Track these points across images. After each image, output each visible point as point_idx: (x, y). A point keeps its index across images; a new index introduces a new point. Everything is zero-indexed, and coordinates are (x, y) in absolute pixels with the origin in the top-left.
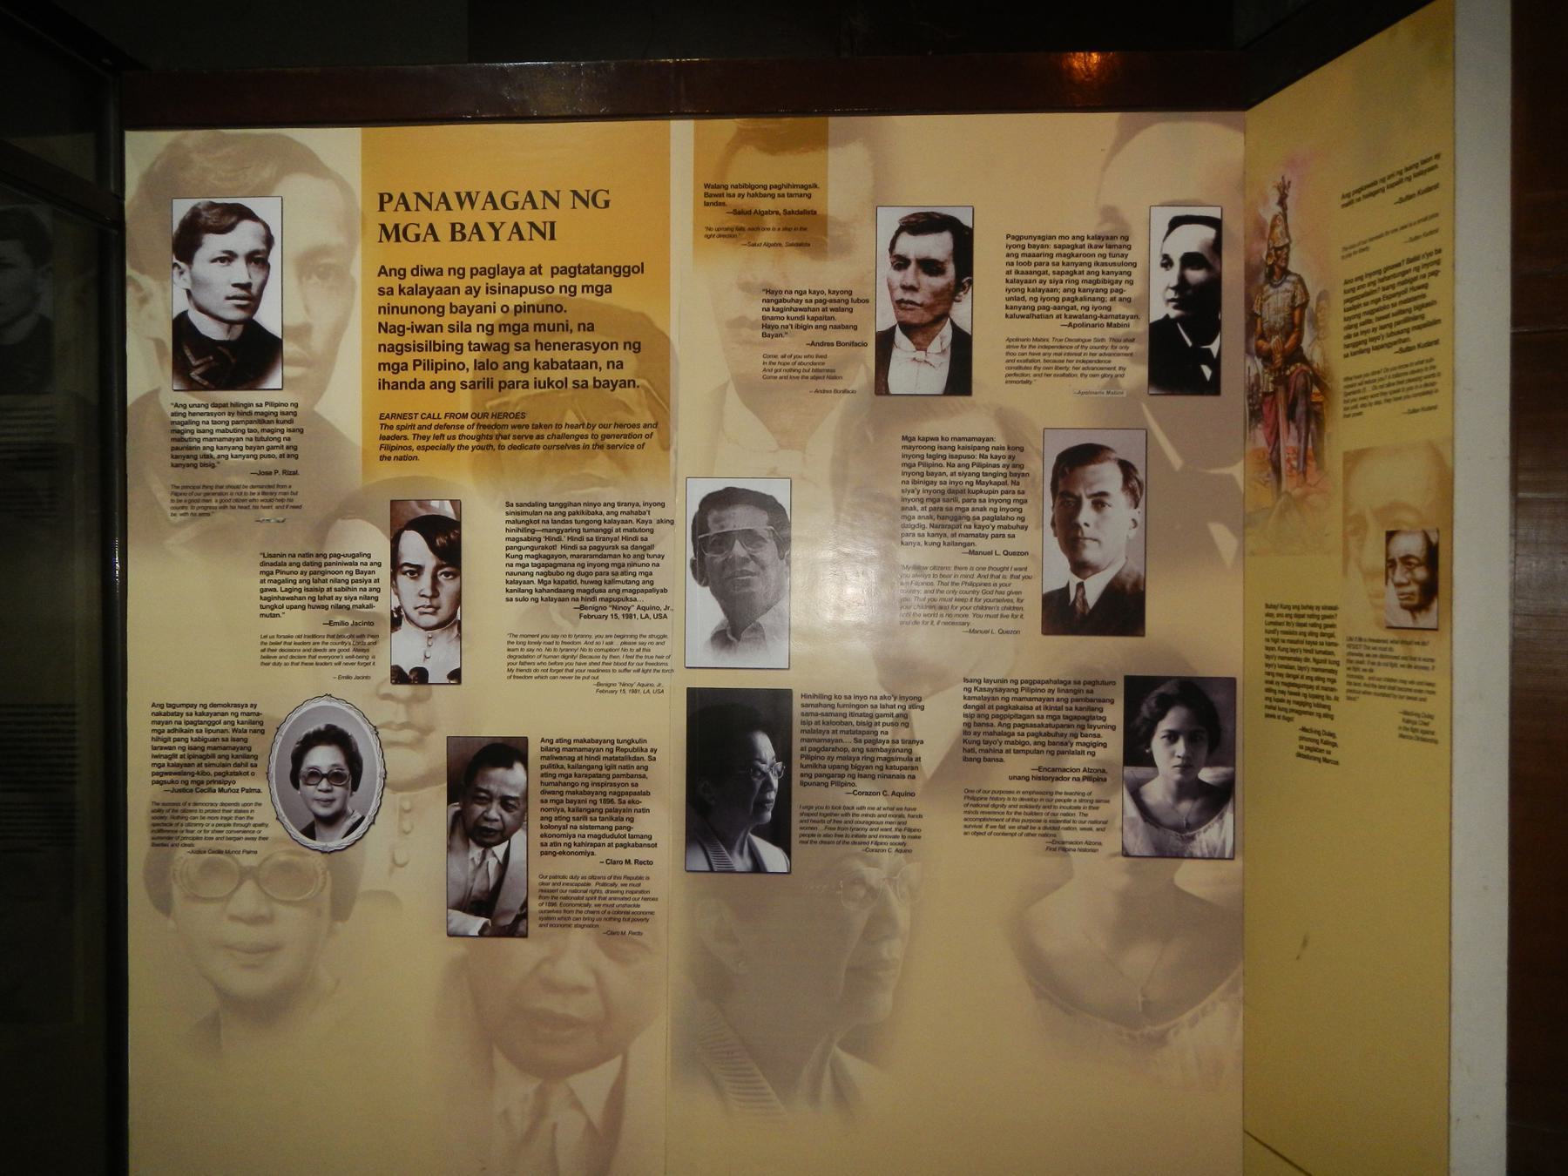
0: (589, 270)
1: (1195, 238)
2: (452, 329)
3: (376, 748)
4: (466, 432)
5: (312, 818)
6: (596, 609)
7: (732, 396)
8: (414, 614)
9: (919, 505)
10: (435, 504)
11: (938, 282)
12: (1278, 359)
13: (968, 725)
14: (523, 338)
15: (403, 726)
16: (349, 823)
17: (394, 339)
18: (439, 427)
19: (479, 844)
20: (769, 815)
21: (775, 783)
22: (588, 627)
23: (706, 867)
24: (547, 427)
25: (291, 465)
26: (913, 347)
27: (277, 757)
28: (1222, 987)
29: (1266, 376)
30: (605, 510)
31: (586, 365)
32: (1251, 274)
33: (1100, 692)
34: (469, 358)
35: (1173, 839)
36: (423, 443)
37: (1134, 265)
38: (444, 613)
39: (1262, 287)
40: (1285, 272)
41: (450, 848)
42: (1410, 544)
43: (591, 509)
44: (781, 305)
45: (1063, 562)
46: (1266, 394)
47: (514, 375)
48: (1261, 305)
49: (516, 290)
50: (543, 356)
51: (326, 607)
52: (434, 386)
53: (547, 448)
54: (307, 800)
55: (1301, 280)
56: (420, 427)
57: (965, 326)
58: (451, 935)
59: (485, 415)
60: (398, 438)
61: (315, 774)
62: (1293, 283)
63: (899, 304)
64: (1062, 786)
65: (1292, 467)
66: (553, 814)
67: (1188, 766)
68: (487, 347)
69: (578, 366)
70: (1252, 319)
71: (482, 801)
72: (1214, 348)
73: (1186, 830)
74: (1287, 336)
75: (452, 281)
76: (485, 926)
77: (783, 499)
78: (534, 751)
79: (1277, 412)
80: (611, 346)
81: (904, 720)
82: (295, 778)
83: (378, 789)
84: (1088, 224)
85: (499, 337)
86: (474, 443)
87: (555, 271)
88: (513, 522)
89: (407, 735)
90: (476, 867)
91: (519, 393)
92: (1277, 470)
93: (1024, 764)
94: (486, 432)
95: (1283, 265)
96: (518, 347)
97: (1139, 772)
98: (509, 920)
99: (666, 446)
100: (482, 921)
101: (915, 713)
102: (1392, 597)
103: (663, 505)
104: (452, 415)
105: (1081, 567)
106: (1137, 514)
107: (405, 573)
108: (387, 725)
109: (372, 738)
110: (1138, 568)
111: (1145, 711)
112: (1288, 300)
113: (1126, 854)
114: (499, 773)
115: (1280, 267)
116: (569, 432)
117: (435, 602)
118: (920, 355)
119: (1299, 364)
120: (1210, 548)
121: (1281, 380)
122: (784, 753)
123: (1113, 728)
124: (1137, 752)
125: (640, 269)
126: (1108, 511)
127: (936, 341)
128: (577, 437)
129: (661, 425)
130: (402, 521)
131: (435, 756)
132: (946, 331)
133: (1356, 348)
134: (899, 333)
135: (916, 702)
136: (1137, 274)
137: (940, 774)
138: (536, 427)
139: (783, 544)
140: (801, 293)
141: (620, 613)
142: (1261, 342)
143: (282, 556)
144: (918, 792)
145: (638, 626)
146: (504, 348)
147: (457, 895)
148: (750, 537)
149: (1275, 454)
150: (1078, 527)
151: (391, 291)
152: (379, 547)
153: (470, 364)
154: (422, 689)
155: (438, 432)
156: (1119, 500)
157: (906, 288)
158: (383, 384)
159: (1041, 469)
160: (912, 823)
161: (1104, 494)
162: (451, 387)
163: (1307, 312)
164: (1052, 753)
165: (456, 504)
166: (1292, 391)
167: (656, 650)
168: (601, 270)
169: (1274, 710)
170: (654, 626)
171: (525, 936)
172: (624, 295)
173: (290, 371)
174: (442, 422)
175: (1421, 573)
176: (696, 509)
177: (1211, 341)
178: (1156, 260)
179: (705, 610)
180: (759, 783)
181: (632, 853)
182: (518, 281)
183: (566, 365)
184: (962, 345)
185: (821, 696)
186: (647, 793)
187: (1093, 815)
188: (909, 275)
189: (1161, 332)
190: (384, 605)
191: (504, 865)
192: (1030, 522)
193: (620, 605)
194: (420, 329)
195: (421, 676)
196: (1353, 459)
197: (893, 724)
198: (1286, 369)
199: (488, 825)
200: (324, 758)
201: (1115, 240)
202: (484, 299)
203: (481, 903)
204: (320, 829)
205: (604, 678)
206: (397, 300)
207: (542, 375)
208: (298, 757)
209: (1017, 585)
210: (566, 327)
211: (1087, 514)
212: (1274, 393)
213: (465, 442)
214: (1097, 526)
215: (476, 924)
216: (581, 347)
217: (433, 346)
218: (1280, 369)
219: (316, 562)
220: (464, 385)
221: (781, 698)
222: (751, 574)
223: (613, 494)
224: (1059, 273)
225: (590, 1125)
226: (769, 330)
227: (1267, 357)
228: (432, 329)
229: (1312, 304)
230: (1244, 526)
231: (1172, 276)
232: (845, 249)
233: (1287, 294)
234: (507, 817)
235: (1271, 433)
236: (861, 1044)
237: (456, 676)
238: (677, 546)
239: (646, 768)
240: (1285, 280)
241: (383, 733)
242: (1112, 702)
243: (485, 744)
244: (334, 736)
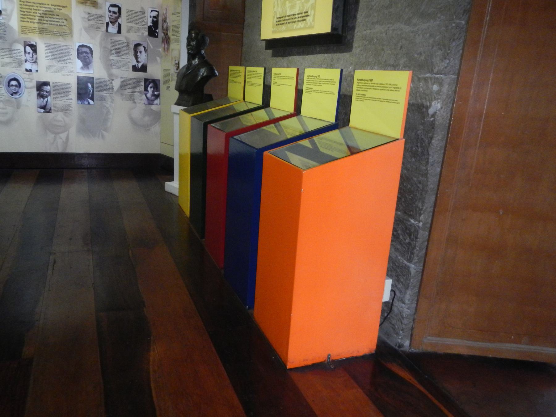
0: (58, 6)
1: (155, 14)
2: (34, 13)
3: (23, 82)
4: (37, 31)
5: (12, 93)
6: (61, 62)
7: (83, 31)
8: (29, 60)
9: (113, 50)
10: (32, 42)
11: (116, 15)
12: (165, 34)
13: (121, 84)
14: (46, 16)
15: (28, 78)
16: (19, 94)
17: (23, 13)
18: (32, 29)
19: (42, 98)
20: (90, 96)
21: (91, 91)
22: (60, 65)
23: (81, 103)
24: (51, 31)
25: (5, 33)
26: (112, 25)
27: (5, 82)
28: (157, 123)
30: (62, 46)
31: (58, 22)
32: (163, 21)
33: (141, 80)
34: (37, 18)
35: (151, 102)
36: (29, 31)
37: (146, 17)
38: (34, 60)
41: (37, 99)
42: (177, 62)
43: (59, 46)
44: (91, 16)
45: (135, 61)
47: (45, 22)
49: (45, 8)
50: (50, 19)
51: (12, 58)
52: (31, 22)
53: (52, 35)
54: (11, 89)
55: (168, 24)
56: (29, 29)
57: (120, 22)
58: (38, 112)
59: (40, 28)
60: (24, 30)
61: (12, 85)
63: (110, 18)
64: (135, 94)
66: (55, 94)
67: (153, 92)
68: (40, 17)
69: (56, 22)
70: (163, 27)
71: (42, 91)
72: (157, 31)
73: (153, 101)
75: (33, 5)
76: (44, 111)
77: (92, 47)
78: (51, 84)
80: (62, 19)
81: (111, 83)
82: (9, 86)
83: (24, 88)
84: (139, 9)
85: (42, 15)
86: (38, 33)
87: (52, 5)
88: (46, 47)
89: (29, 80)
90: (42, 102)
91: (46, 25)
92: (165, 50)
93: (130, 90)
94: (41, 31)
96: (46, 17)
97: (147, 92)
98: (48, 110)
99: (72, 36)
100: (44, 110)
101: (113, 82)
102: (175, 69)
103: (71, 46)
104: (34, 28)
105: (138, 62)
106: (146, 54)
107: (27, 53)
108: (25, 78)
109: (22, 80)
110: (146, 63)
111: (147, 83)
113: (144, 104)
114: (45, 87)
116: (56, 33)
117: (33, 58)
118: (113, 27)
120: (156, 60)
121: (166, 37)
122: (93, 87)
123: (142, 86)
124: (146, 89)
125: (67, 7)
126: (142, 54)
127: (116, 25)
128: (57, 34)
129: (71, 33)
130: (26, 44)
131: (34, 84)
132: (117, 23)
133: (173, 35)
134: (110, 23)
135: (113, 80)
136: (146, 18)
137: (117, 91)
138: (50, 31)
139: (92, 54)
140: (94, 14)
141: (65, 63)
143: (4, 48)
144: (113, 93)
145: (68, 65)
146: (43, 17)
147: (39, 106)
148: (86, 53)
150: (137, 56)
151: (22, 5)
152: (22, 49)
153: (37, 19)
154: (31, 73)
155: (32, 30)
156: (143, 52)
157: (111, 16)
158: (21, 21)
159: (132, 47)
160: (113, 98)
161: (141, 51)
162: (34, 23)
164: (134, 89)
165: (36, 43)
167: (71, 69)
168: (60, 6)
169: (164, 84)
170: (71, 65)
171: (51, 113)
172: (64, 11)
173: (3, 16)
174: (32, 28)
175: (178, 65)
176: (77, 47)
177: (157, 30)
178: (149, 16)
179: (79, 64)
180: (89, 91)
181: (68, 101)
182: (45, 6)
183: (54, 21)
184: (120, 26)
185: (99, 78)
186: (71, 92)
187: (140, 98)
188: (111, 14)
189: (150, 27)
190: (23, 58)
191: (47, 102)
192: (130, 54)
193: (64, 61)
194: (28, 12)
195: (31, 71)
196: (172, 50)
197: (110, 83)
199: (44, 95)
200: (14, 83)
201: (143, 12)
202: (39, 8)
203: (44, 107)
204: (14, 94)
205: (63, 73)
206: (23, 6)
207: (50, 23)
208: (9, 82)
209: (128, 64)
210: (54, 15)
211: (139, 54)
213: (37, 32)
214: (140, 56)
215: (43, 110)
216: (57, 18)
217: (30, 15)
219: (10, 50)
220: (36, 23)
221: (93, 78)
222: (86, 58)
223: (63, 44)
224: (135, 16)
225: (63, 141)
226: (89, 20)
227: (164, 33)
228: (30, 12)
229: (169, 27)
230: (161, 58)
231: (151, 19)
232: (101, 8)
234: (47, 94)
236: (105, 130)
237: (37, 71)
238: (75, 53)
239: (70, 88)
241: (24, 79)
242: (142, 82)
243: (41, 83)
244: (15, 79)
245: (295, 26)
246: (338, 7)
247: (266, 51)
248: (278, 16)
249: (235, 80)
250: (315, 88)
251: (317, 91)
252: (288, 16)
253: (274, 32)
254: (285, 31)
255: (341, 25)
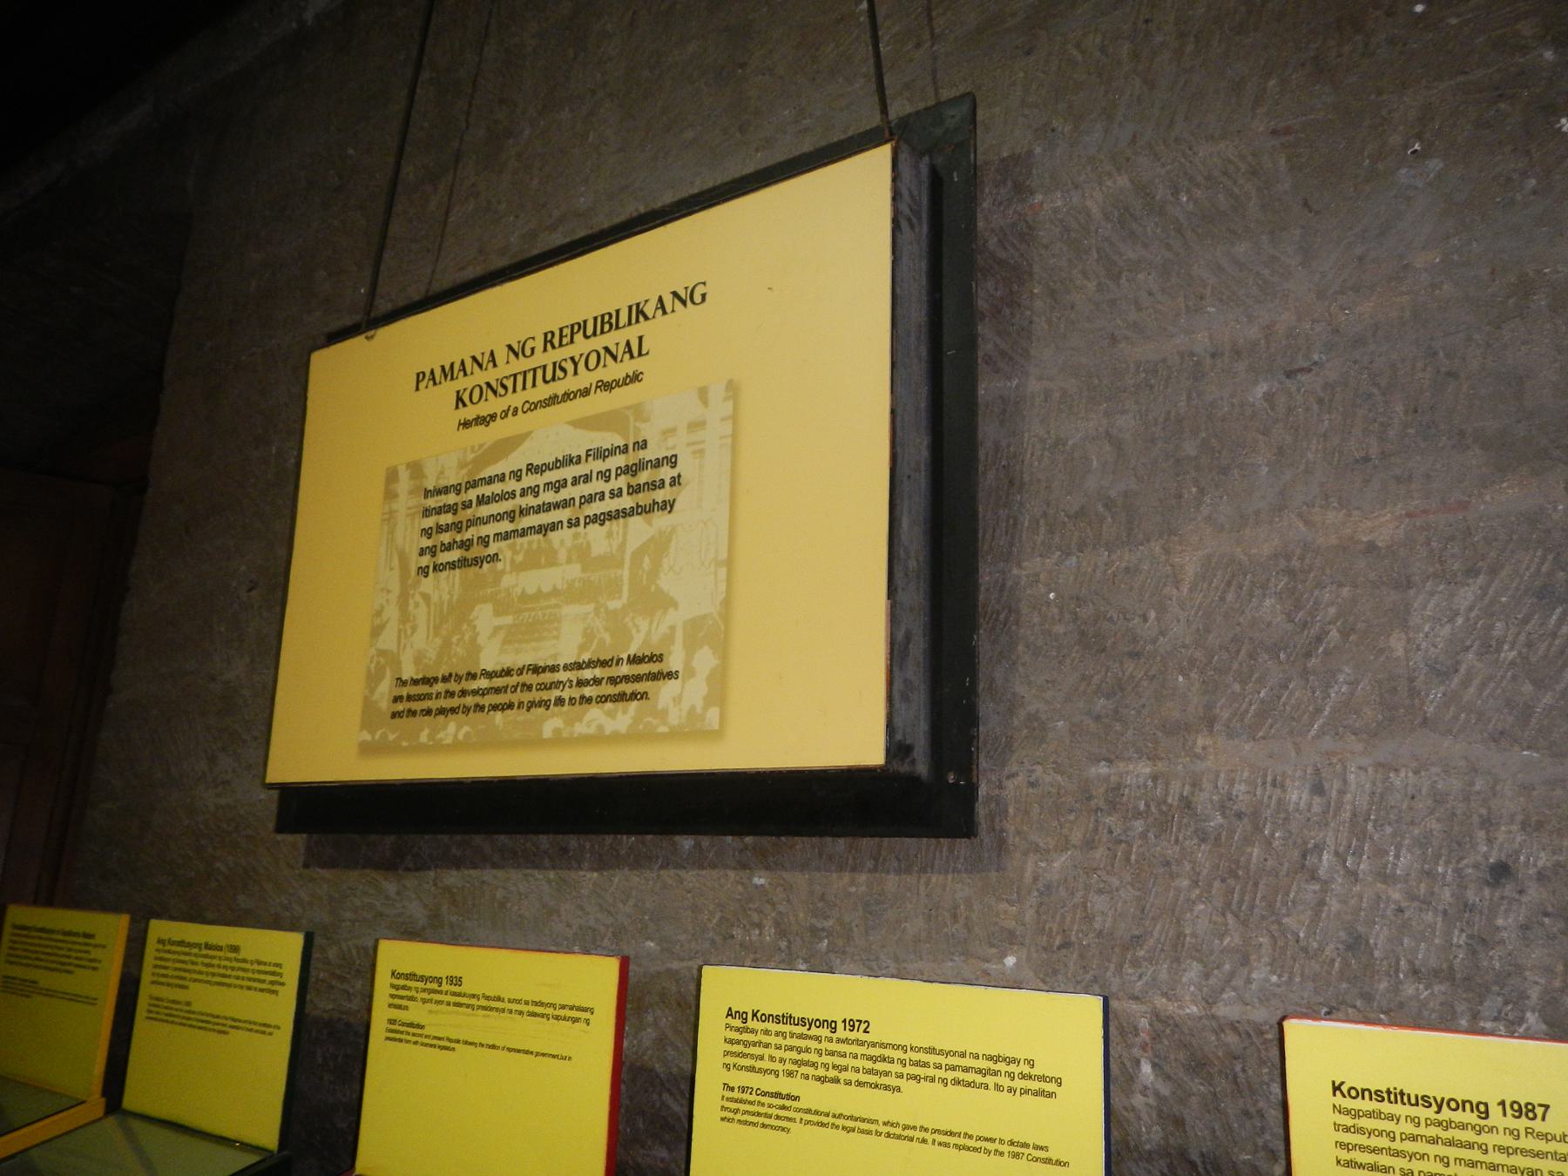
245: (552, 723)
246: (908, 637)
247: (280, 837)
248: (408, 672)
249: (45, 979)
250: (813, 1095)
251: (821, 1119)
252: (489, 675)
253: (366, 750)
254: (457, 747)
255: (923, 727)
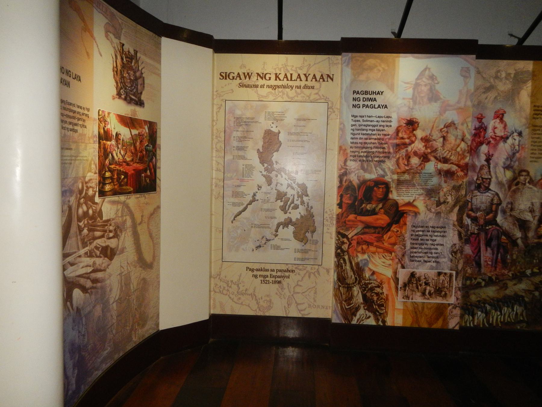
12: (482, 222)
29: (473, 226)
39: (472, 191)
40: (487, 189)
46: (472, 234)
48: (472, 198)
62: (493, 194)
65: (488, 264)
74: (488, 214)
79: (479, 243)
95: (487, 185)
112: (489, 200)
115: (485, 186)
119: (494, 226)
121: (482, 229)
142: (470, 212)
149: (477, 257)
163: (500, 207)
166: (489, 235)
198: (486, 226)
212: (478, 234)
218: (482, 226)
233: (488, 198)
235: (475, 249)
240: (487, 192)
